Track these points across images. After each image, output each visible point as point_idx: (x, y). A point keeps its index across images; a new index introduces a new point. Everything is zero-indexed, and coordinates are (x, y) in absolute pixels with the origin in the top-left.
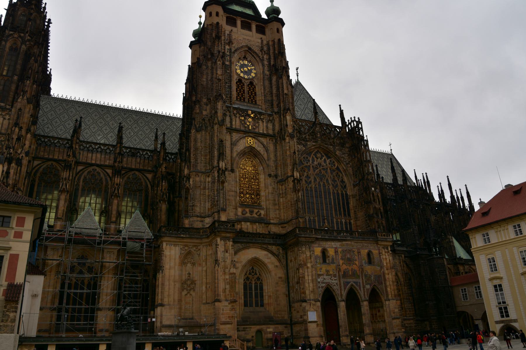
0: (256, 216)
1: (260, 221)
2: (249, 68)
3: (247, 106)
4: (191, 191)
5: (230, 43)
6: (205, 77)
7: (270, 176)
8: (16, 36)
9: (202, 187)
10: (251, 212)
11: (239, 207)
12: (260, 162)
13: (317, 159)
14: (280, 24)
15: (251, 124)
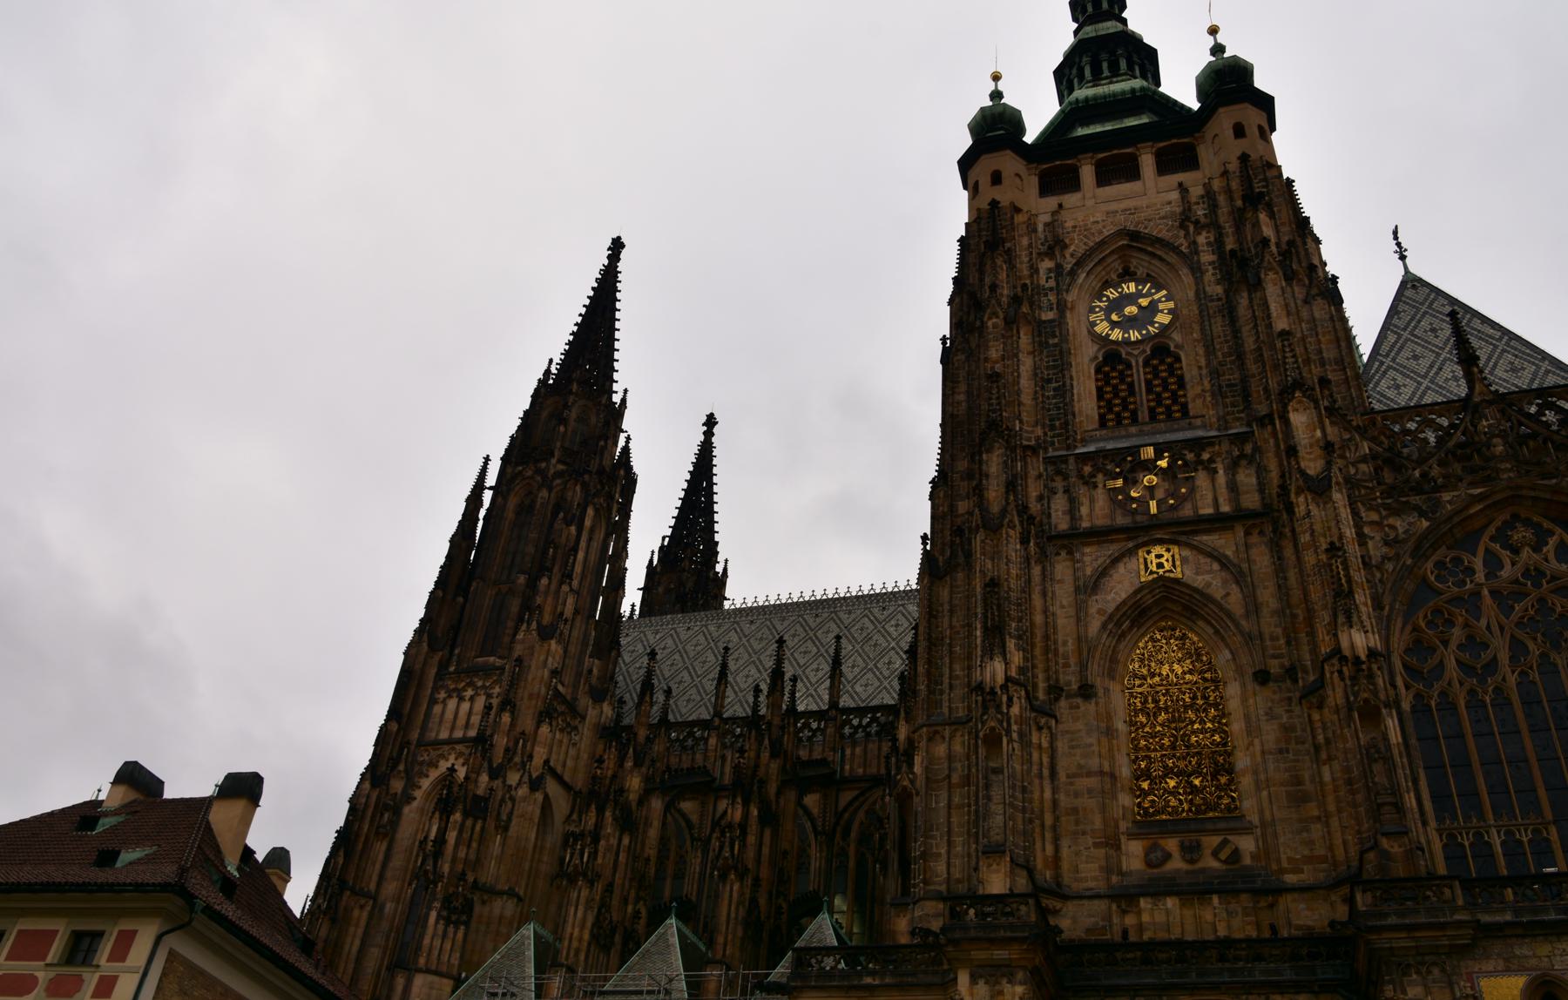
0: (1215, 864)
1: (1237, 883)
2: (1144, 302)
3: (1141, 433)
4: (916, 800)
5: (1055, 245)
6: (963, 387)
7: (1262, 677)
8: (530, 473)
9: (955, 779)
10: (1191, 851)
11: (1132, 836)
12: (1217, 632)
13: (1516, 551)
14: (1246, 105)
15: (1160, 494)
